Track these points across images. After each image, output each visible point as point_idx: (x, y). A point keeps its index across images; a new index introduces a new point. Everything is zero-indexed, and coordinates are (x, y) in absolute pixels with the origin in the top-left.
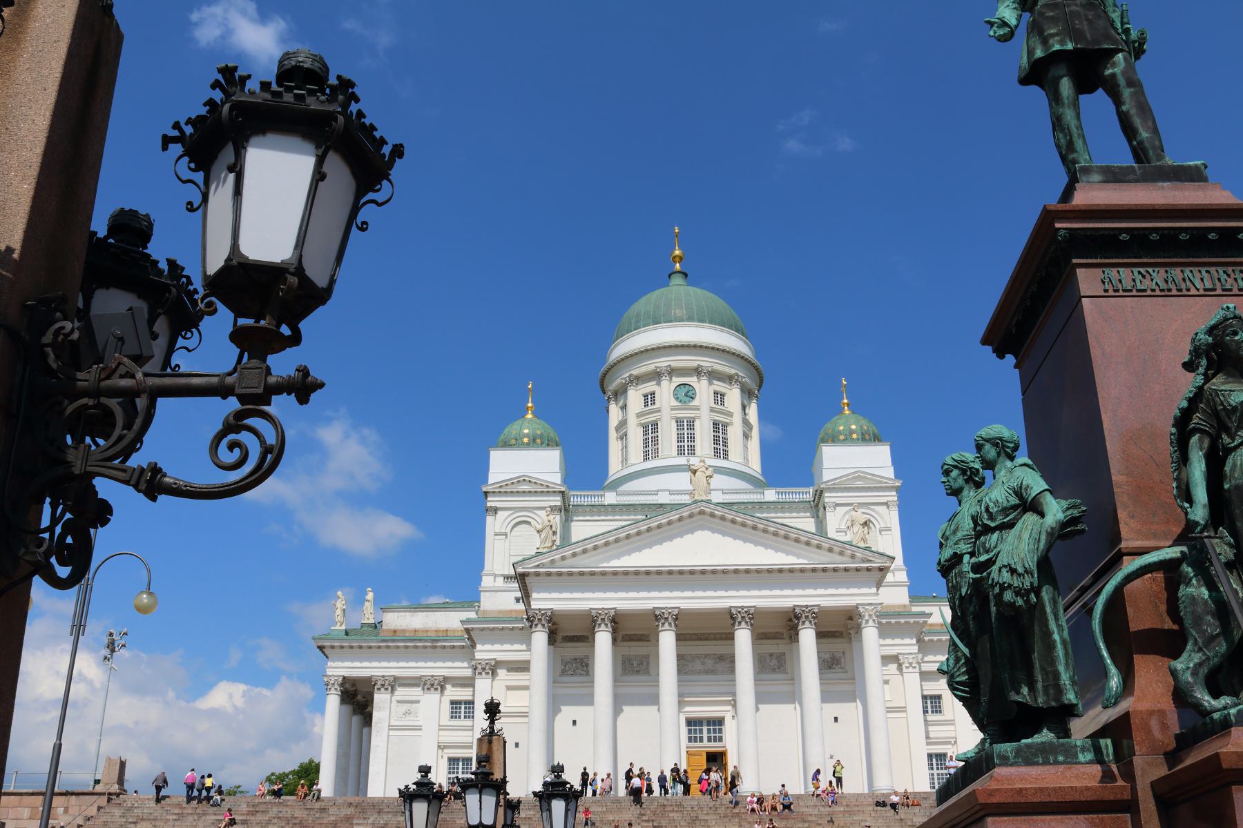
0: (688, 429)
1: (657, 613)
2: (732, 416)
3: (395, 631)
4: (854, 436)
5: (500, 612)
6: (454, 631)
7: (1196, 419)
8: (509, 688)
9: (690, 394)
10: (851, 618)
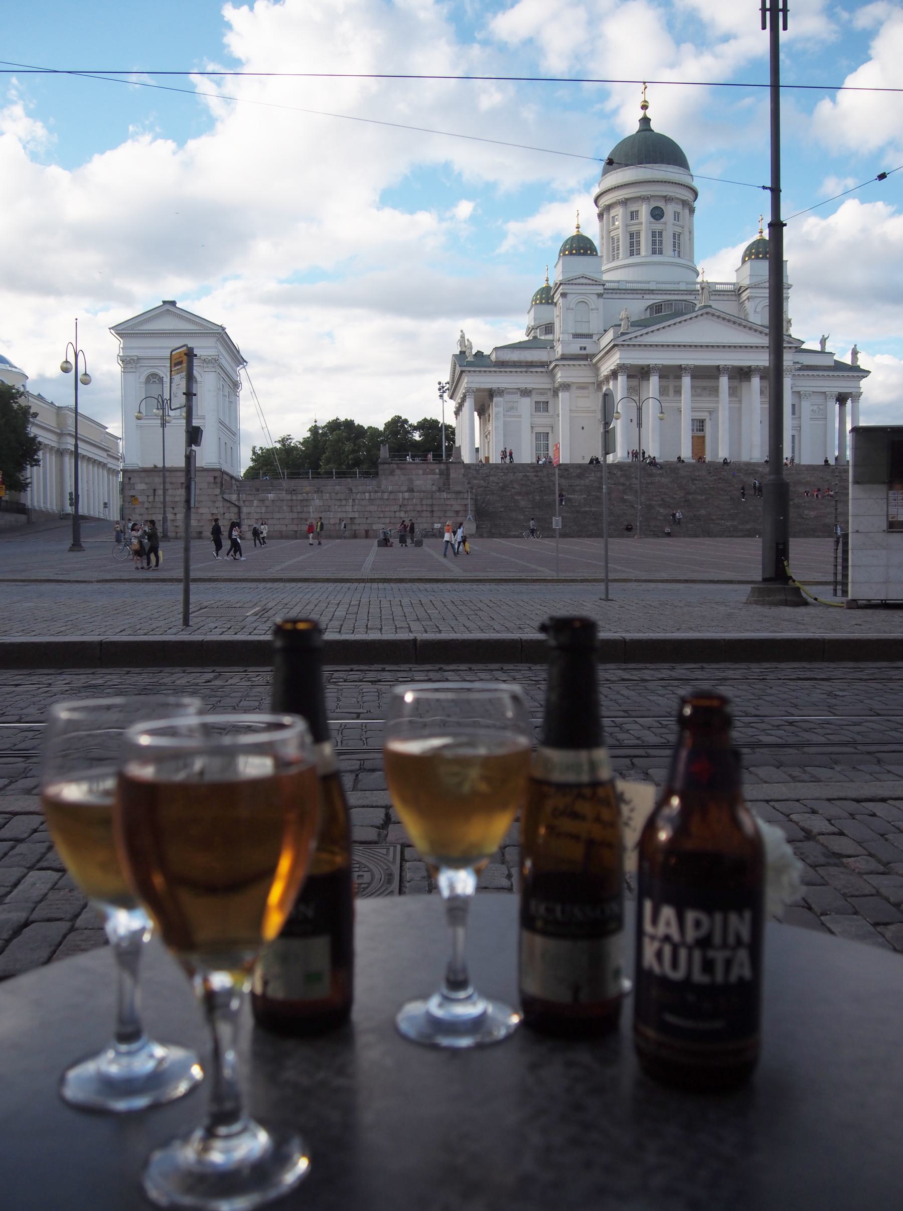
1: (683, 366)
3: (503, 362)
5: (573, 355)
6: (536, 362)
8: (578, 397)
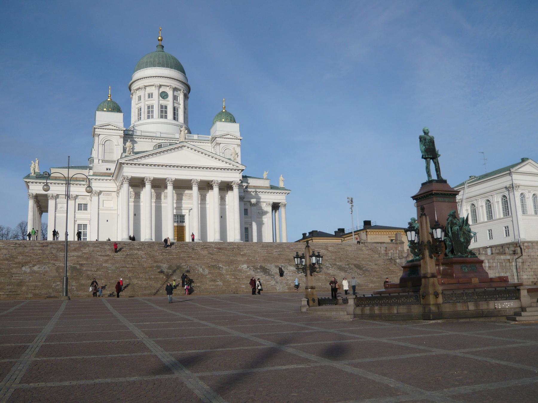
0: (165, 109)
2: (180, 105)
4: (228, 120)
5: (101, 173)
7: (449, 224)
9: (166, 96)
10: (228, 184)
